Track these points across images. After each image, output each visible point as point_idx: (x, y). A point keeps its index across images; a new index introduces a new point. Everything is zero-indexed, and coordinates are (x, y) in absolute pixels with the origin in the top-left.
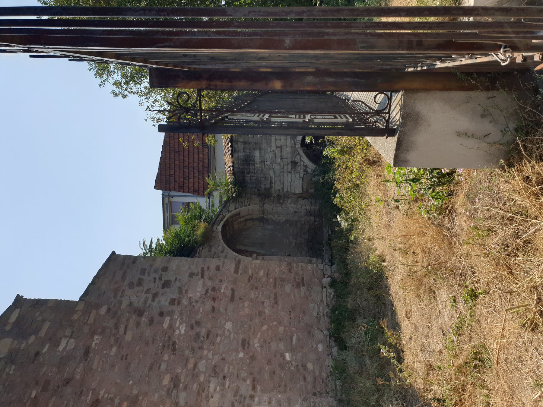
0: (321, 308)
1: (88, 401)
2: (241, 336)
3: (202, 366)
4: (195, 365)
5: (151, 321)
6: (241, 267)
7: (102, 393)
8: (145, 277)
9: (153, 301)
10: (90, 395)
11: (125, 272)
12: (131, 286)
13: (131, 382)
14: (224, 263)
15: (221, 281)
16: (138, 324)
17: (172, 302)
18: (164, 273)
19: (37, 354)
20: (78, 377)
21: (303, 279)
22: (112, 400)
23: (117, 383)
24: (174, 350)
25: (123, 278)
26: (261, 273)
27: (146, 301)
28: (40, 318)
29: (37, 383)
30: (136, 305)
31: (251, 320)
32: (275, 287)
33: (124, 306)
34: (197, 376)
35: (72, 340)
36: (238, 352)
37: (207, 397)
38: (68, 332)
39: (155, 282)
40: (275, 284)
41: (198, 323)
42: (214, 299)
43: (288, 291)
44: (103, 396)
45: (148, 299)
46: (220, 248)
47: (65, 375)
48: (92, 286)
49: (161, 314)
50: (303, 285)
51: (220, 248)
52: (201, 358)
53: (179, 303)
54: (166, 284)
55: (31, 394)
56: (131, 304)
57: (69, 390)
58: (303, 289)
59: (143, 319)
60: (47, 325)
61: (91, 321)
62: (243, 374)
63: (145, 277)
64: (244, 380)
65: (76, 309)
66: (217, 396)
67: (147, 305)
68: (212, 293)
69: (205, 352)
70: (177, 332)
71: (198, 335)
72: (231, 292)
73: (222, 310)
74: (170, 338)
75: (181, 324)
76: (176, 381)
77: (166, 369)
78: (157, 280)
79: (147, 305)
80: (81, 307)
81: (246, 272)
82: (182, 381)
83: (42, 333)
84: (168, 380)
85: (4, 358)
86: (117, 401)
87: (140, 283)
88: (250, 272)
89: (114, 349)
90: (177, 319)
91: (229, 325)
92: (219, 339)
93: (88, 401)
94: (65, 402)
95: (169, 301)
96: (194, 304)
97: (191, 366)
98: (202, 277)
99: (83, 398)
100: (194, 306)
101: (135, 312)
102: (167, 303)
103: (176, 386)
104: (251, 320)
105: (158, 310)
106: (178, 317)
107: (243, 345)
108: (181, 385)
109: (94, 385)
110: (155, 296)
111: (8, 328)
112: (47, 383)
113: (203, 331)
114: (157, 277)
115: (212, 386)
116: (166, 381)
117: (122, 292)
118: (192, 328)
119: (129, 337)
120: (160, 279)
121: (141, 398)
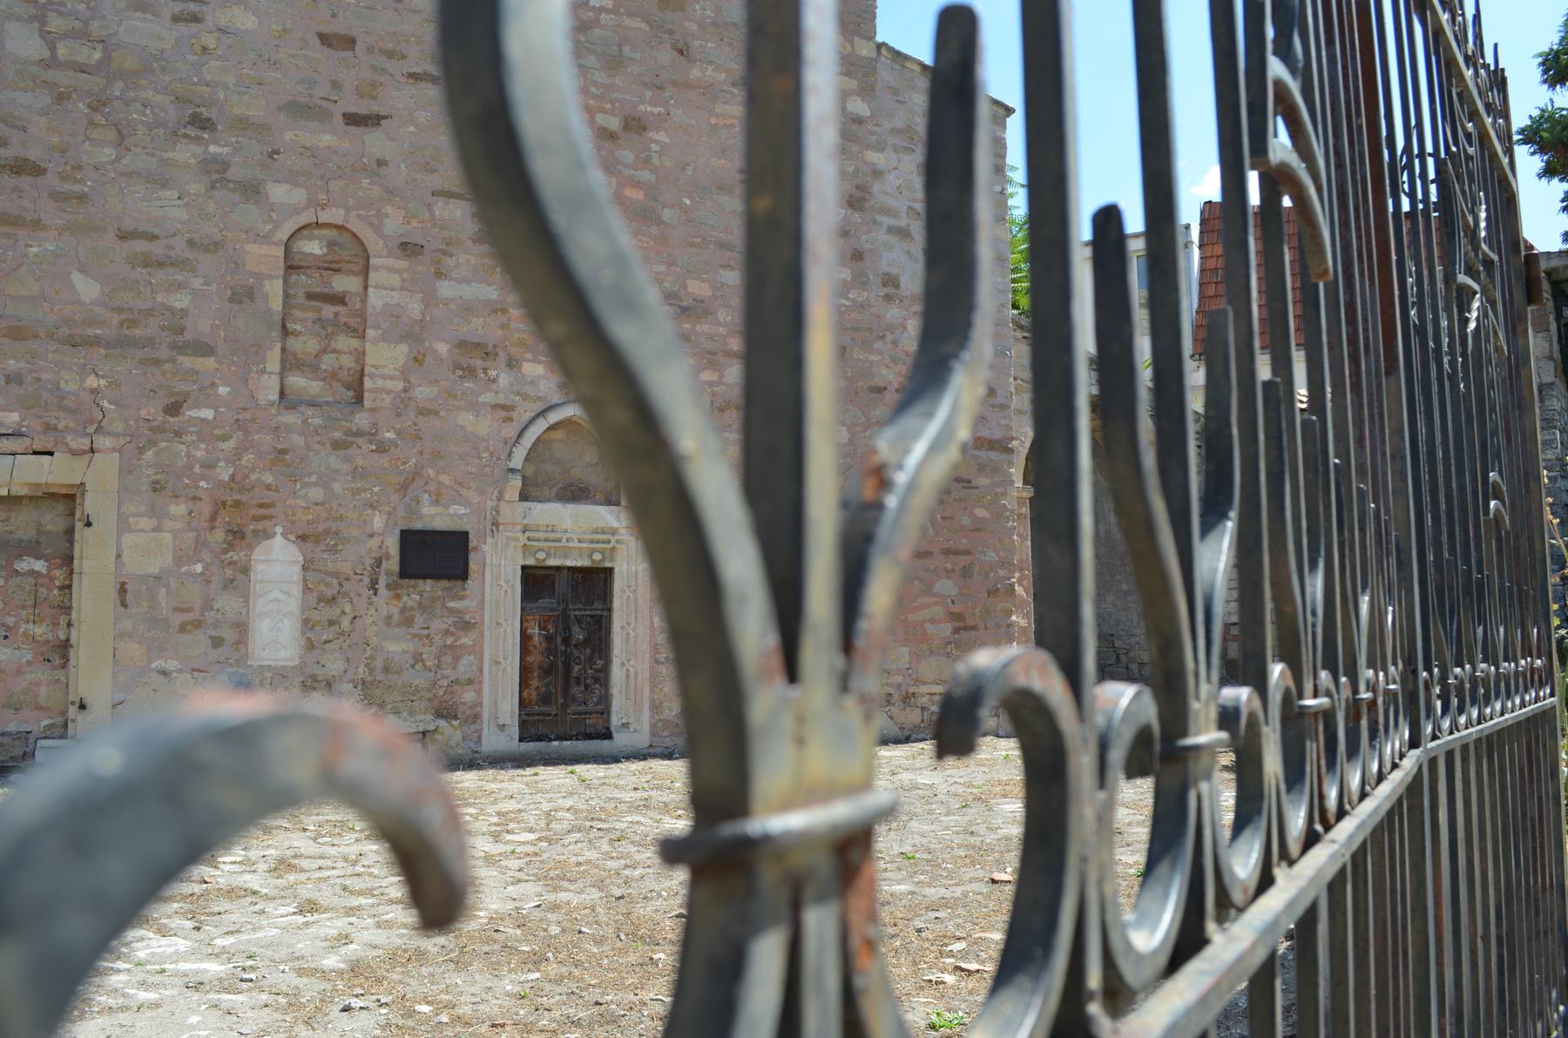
0: (899, 679)
1: (642, 107)
6: (993, 455)
7: (661, 137)
9: (890, 230)
10: (656, 110)
13: (688, 202)
20: (695, 73)
21: (974, 628)
23: (684, 169)
27: (887, 212)
30: (876, 188)
32: (947, 552)
40: (956, 553)
43: (937, 588)
44: (656, 142)
45: (895, 217)
47: (697, 43)
48: (917, 68)
50: (956, 631)
53: (888, 298)
57: (665, 56)
58: (947, 629)
65: (856, 39)
67: (878, 217)
77: (723, 284)
79: (878, 217)
80: (865, 50)
81: (982, 469)
82: (698, 328)
84: (698, 292)
86: (645, 175)
88: (983, 481)
90: (848, 299)
93: (642, 107)
94: (638, 56)
95: (894, 271)
96: (889, 337)
99: (649, 94)
100: (882, 338)
101: (858, 187)
102: (886, 268)
105: (866, 246)
106: (853, 300)
108: (687, 326)
109: (678, 114)
121: (654, 230)
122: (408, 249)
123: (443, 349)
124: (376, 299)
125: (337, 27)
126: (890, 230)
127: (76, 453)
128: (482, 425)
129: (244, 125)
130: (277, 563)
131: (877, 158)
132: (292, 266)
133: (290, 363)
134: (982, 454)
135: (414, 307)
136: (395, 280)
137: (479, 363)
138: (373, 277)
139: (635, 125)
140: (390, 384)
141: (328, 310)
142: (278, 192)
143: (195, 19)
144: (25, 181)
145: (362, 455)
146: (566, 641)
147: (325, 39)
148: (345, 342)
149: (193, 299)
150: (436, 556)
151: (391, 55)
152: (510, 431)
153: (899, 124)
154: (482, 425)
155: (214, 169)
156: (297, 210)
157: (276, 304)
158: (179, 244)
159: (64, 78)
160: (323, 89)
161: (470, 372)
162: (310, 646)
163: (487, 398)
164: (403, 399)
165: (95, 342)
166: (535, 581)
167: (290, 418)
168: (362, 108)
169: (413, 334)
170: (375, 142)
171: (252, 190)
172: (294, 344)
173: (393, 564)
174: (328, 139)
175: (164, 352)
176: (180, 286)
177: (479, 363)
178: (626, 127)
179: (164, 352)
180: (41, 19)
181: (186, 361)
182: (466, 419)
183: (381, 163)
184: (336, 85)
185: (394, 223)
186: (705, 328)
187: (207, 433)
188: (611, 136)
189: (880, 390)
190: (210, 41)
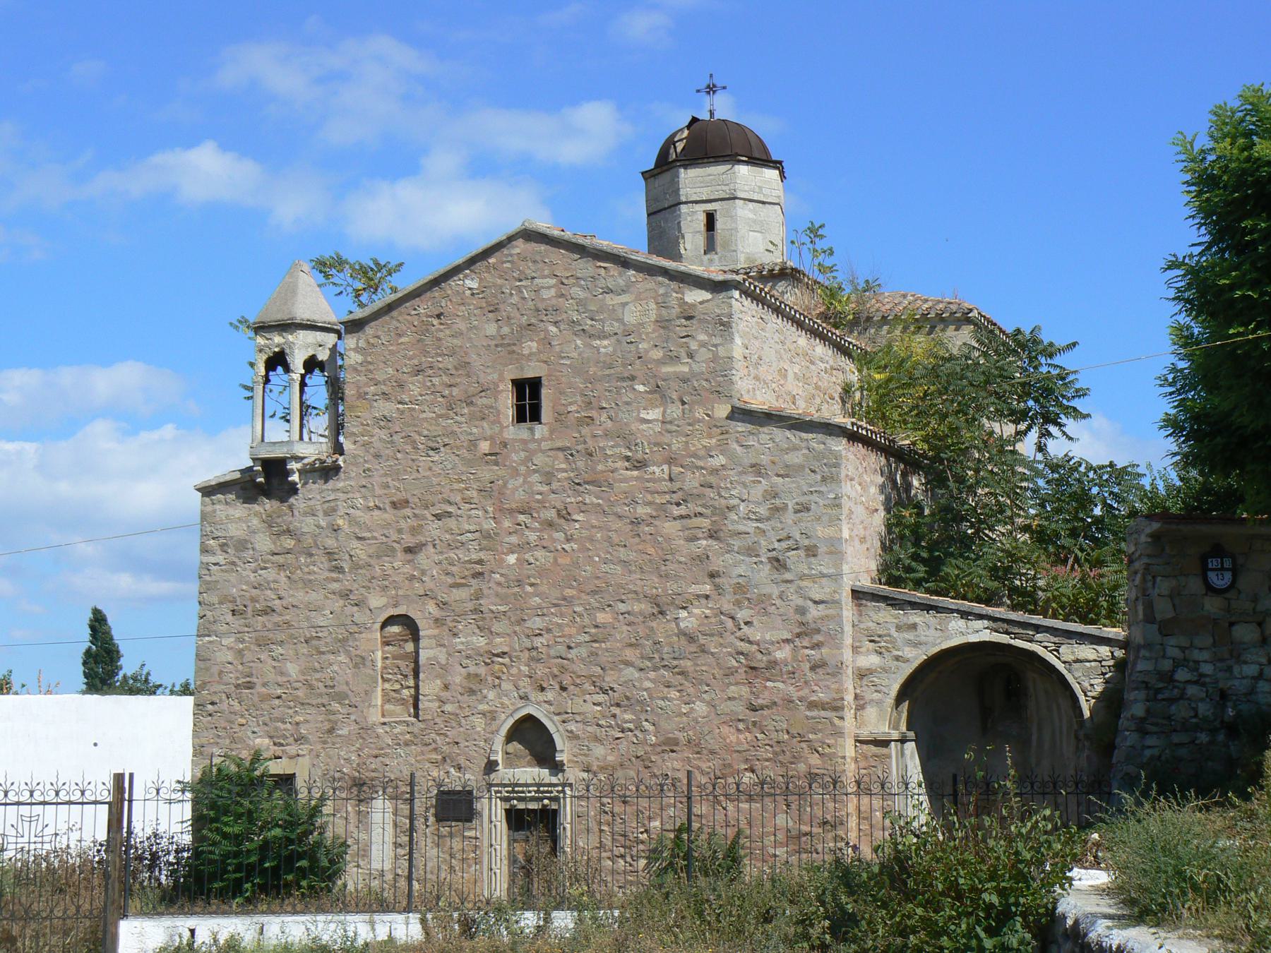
4: (628, 663)
6: (823, 713)
16: (694, 539)
19: (632, 378)
39: (779, 541)
46: (908, 652)
49: (712, 575)
51: (908, 652)
54: (778, 564)
55: (571, 404)
59: (704, 542)
61: (697, 445)
63: (789, 517)
70: (683, 614)
72: (764, 702)
78: (784, 545)
85: (624, 324)
89: (649, 510)
97: (630, 654)
98: (798, 635)
110: (751, 551)
117: (754, 482)
119: (670, 527)
120: (790, 549)
127: (291, 758)
130: (381, 811)
134: (814, 713)
138: (422, 643)
140: (431, 705)
142: (376, 601)
147: (394, 505)
153: (747, 462)
159: (280, 559)
161: (472, 692)
166: (516, 820)
184: (400, 531)
187: (348, 740)
188: (550, 524)
189: (730, 672)
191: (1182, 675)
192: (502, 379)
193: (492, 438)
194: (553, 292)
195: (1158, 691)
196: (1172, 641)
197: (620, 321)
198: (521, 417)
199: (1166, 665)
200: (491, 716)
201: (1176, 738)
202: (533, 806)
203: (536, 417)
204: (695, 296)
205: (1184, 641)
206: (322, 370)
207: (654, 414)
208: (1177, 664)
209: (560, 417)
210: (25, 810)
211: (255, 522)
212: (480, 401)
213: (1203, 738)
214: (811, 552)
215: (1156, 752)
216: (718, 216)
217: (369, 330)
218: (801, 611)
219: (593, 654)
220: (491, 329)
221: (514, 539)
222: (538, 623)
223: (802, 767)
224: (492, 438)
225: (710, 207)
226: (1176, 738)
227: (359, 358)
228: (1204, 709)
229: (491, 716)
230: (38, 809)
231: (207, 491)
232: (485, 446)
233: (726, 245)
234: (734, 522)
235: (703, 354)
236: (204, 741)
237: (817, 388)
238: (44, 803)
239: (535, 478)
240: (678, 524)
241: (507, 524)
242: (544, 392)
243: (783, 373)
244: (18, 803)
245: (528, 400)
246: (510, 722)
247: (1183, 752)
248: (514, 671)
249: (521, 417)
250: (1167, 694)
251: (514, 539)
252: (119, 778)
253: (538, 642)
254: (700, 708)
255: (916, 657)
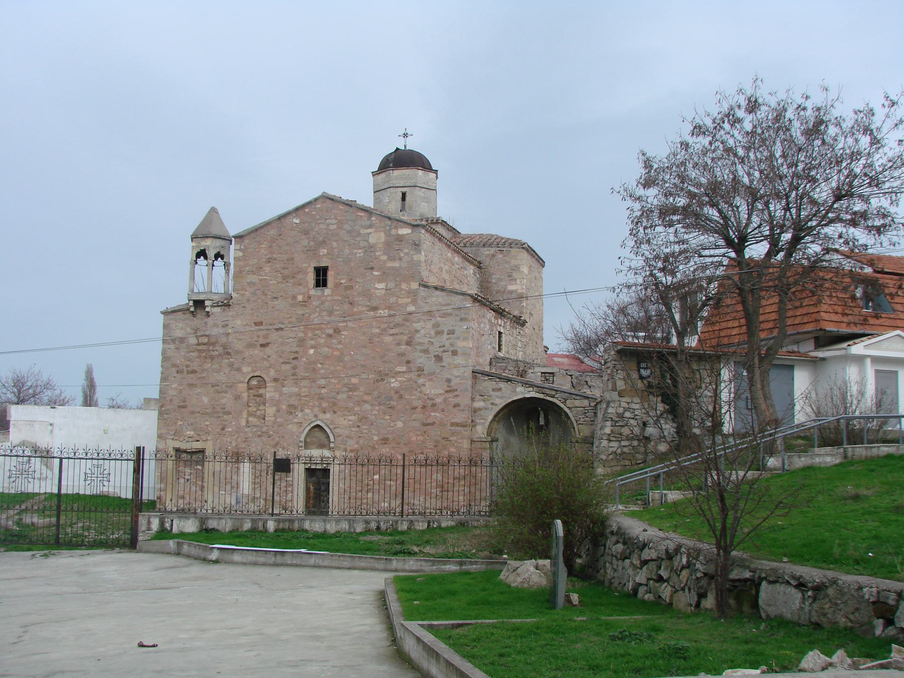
2: (390, 436)
3: (367, 407)
4: (365, 402)
5: (401, 355)
6: (457, 428)
7: (345, 333)
8: (445, 336)
9: (421, 351)
11: (450, 315)
12: (436, 325)
14: (463, 410)
15: (443, 410)
16: (399, 344)
17: (421, 369)
18: (450, 353)
19: (372, 268)
20: (355, 310)
22: (340, 343)
24: (378, 381)
25: (444, 315)
26: (452, 450)
27: (420, 344)
28: (402, 255)
29: (351, 280)
31: (405, 444)
33: (415, 325)
34: (358, 405)
35: (383, 292)
36: (378, 435)
37: (345, 415)
38: (391, 285)
41: (401, 397)
42: (424, 407)
46: (498, 401)
49: (408, 362)
52: (372, 405)
53: (419, 376)
54: (439, 358)
56: (417, 331)
57: (346, 306)
60: (396, 264)
61: (401, 301)
62: (361, 441)
63: (445, 336)
64: (357, 443)
66: (345, 422)
68: (429, 405)
69: (377, 408)
71: (391, 399)
73: (414, 416)
74: (387, 375)
75: (400, 382)
76: (353, 388)
78: (441, 349)
81: (453, 434)
83: (390, 264)
86: (340, 346)
87: (439, 333)
89: (377, 331)
91: (400, 424)
92: (387, 417)
97: (366, 398)
98: (447, 392)
103: (350, 390)
104: (405, 444)
107: (384, 439)
110: (426, 351)
111: (393, 232)
112: (351, 288)
113: (393, 403)
114: (445, 348)
115: (352, 418)
116: (354, 380)
118: (397, 392)
119: (388, 339)
120: (444, 351)
122: (276, 380)
123: (284, 407)
124: (268, 395)
125: (259, 320)
126: (421, 351)
128: (293, 428)
129: (238, 352)
131: (417, 326)
132: (249, 389)
133: (250, 414)
135: (277, 396)
136: (272, 389)
137: (293, 411)
139: (337, 331)
141: (258, 399)
142: (245, 369)
143: (227, 325)
144: (193, 375)
145: (264, 439)
146: (319, 489)
147: (256, 324)
148: (262, 407)
149: (227, 400)
150: (282, 466)
151: (271, 325)
152: (301, 429)
154: (293, 428)
155: (231, 365)
156: (248, 373)
157: (246, 399)
158: (224, 386)
160: (255, 338)
161: (291, 413)
162: (254, 489)
163: (295, 420)
164: (275, 422)
165: (206, 414)
166: (310, 472)
167: (247, 429)
168: (262, 341)
169: (277, 404)
170: (268, 350)
171: (239, 370)
172: (250, 409)
173: (272, 468)
174: (256, 352)
175: (221, 415)
176: (224, 397)
177: (293, 411)
178: (335, 331)
179: (221, 415)
180: (196, 333)
181: (225, 417)
182: (290, 426)
183: (269, 357)
184: (258, 336)
185: (272, 373)
186: (356, 393)
188: (330, 336)
189: (415, 408)
190: (230, 331)
191: (627, 414)
192: (309, 266)
193: (303, 294)
194: (335, 226)
195: (616, 422)
196: (623, 399)
197: (367, 241)
198: (318, 284)
199: (621, 410)
200: (300, 424)
201: (623, 443)
202: (319, 467)
203: (325, 284)
204: (405, 231)
205: (629, 400)
206: (222, 259)
207: (382, 286)
208: (625, 410)
209: (338, 285)
210: (95, 462)
211: (189, 330)
212: (300, 276)
213: (635, 443)
214: (455, 353)
215: (614, 449)
216: (407, 194)
217: (246, 241)
218: (449, 381)
219: (349, 397)
220: (305, 242)
221: (313, 342)
222: (322, 382)
223: (446, 453)
224: (303, 294)
225: (404, 190)
226: (623, 443)
227: (241, 254)
228: (637, 431)
229: (300, 424)
230: (101, 462)
231: (165, 313)
232: (300, 298)
233: (411, 208)
234: (418, 338)
235: (406, 259)
236: (163, 431)
237: (455, 277)
238: (104, 459)
239: (324, 313)
240: (391, 338)
241: (310, 335)
242: (330, 273)
243: (441, 269)
244: (92, 459)
245: (321, 277)
246: (309, 428)
247: (626, 450)
248: (311, 404)
249: (318, 284)
250: (620, 424)
251: (313, 342)
252: (138, 449)
253: (323, 391)
254: (400, 424)
255: (501, 403)
